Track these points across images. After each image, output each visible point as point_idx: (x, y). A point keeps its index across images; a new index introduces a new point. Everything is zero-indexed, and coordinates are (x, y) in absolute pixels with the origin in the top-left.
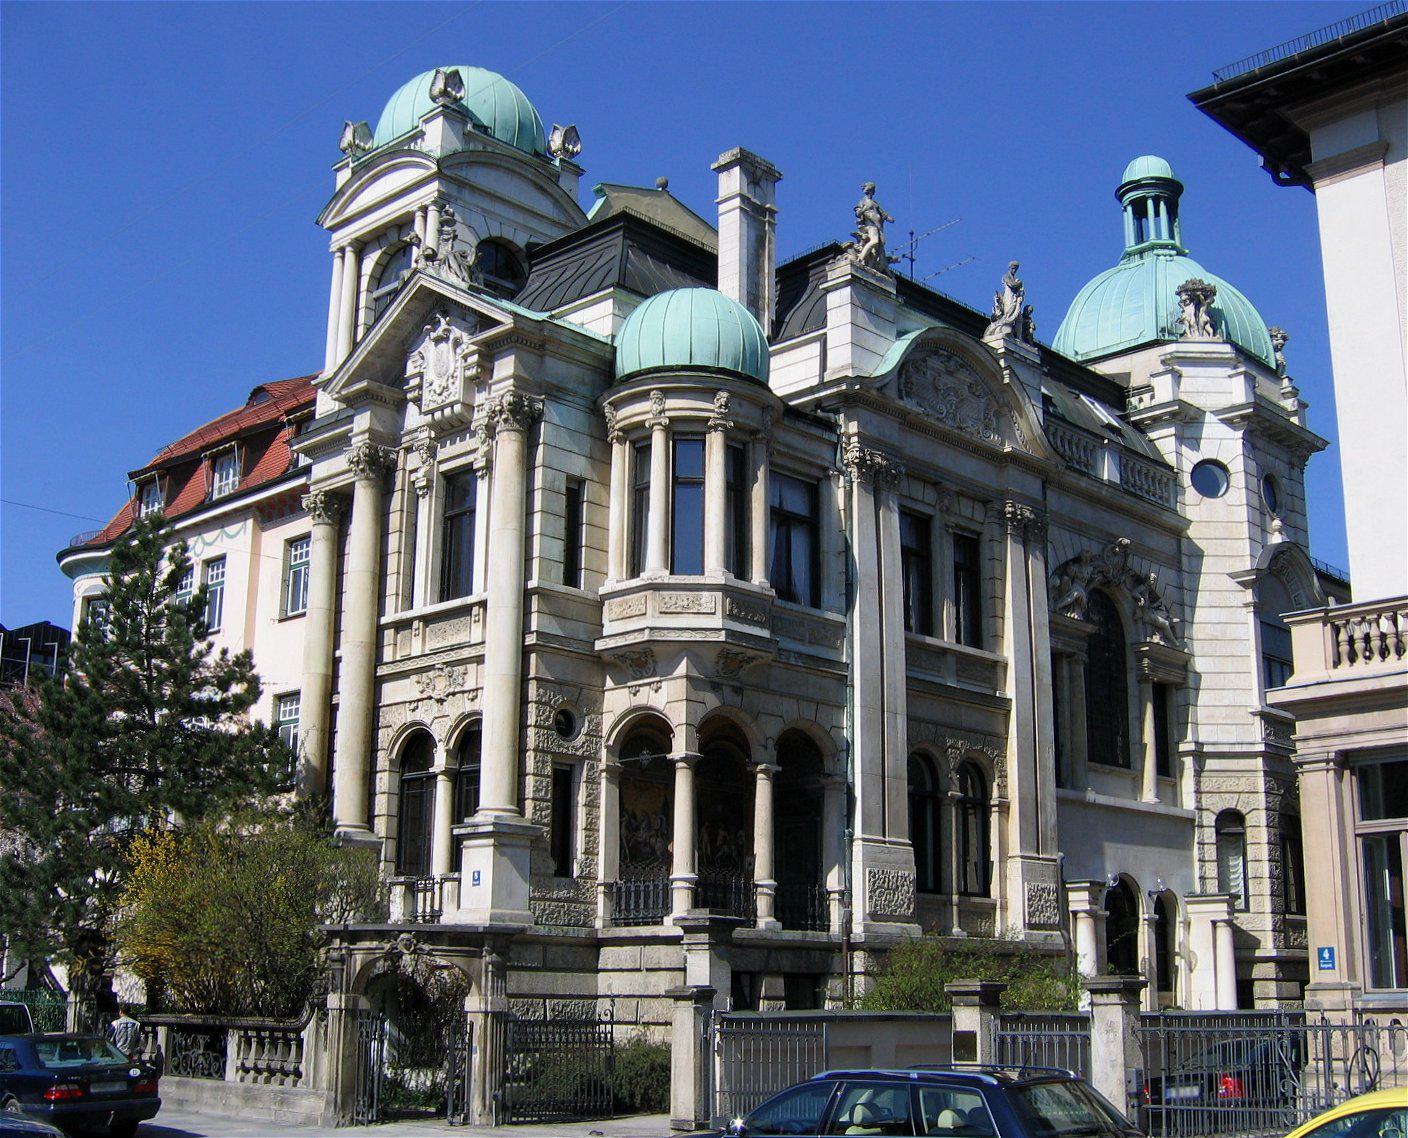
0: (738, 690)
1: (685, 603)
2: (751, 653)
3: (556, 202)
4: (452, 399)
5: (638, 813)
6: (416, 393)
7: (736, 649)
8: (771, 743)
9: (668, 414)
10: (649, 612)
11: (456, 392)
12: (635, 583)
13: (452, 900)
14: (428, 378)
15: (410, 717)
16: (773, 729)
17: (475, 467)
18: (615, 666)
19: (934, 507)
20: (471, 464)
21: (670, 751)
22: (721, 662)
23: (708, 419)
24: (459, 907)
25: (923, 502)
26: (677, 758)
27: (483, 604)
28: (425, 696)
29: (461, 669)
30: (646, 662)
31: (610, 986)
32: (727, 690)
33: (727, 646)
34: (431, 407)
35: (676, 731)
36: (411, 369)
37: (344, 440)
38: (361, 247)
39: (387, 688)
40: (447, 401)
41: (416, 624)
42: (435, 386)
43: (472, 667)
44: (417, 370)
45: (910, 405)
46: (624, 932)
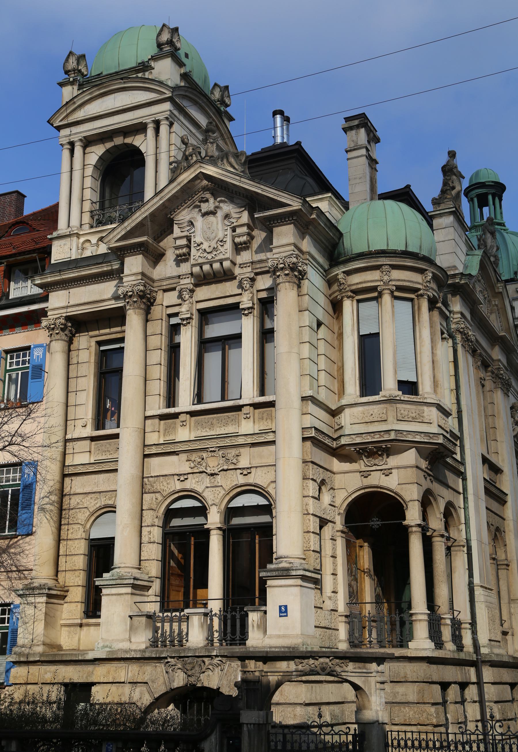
4: (221, 257)
9: (394, 283)
10: (390, 419)
15: (179, 486)
17: (241, 307)
20: (239, 303)
23: (419, 289)
24: (265, 631)
26: (413, 524)
29: (233, 452)
35: (410, 505)
37: (117, 274)
38: (88, 142)
42: (205, 246)
43: (245, 451)
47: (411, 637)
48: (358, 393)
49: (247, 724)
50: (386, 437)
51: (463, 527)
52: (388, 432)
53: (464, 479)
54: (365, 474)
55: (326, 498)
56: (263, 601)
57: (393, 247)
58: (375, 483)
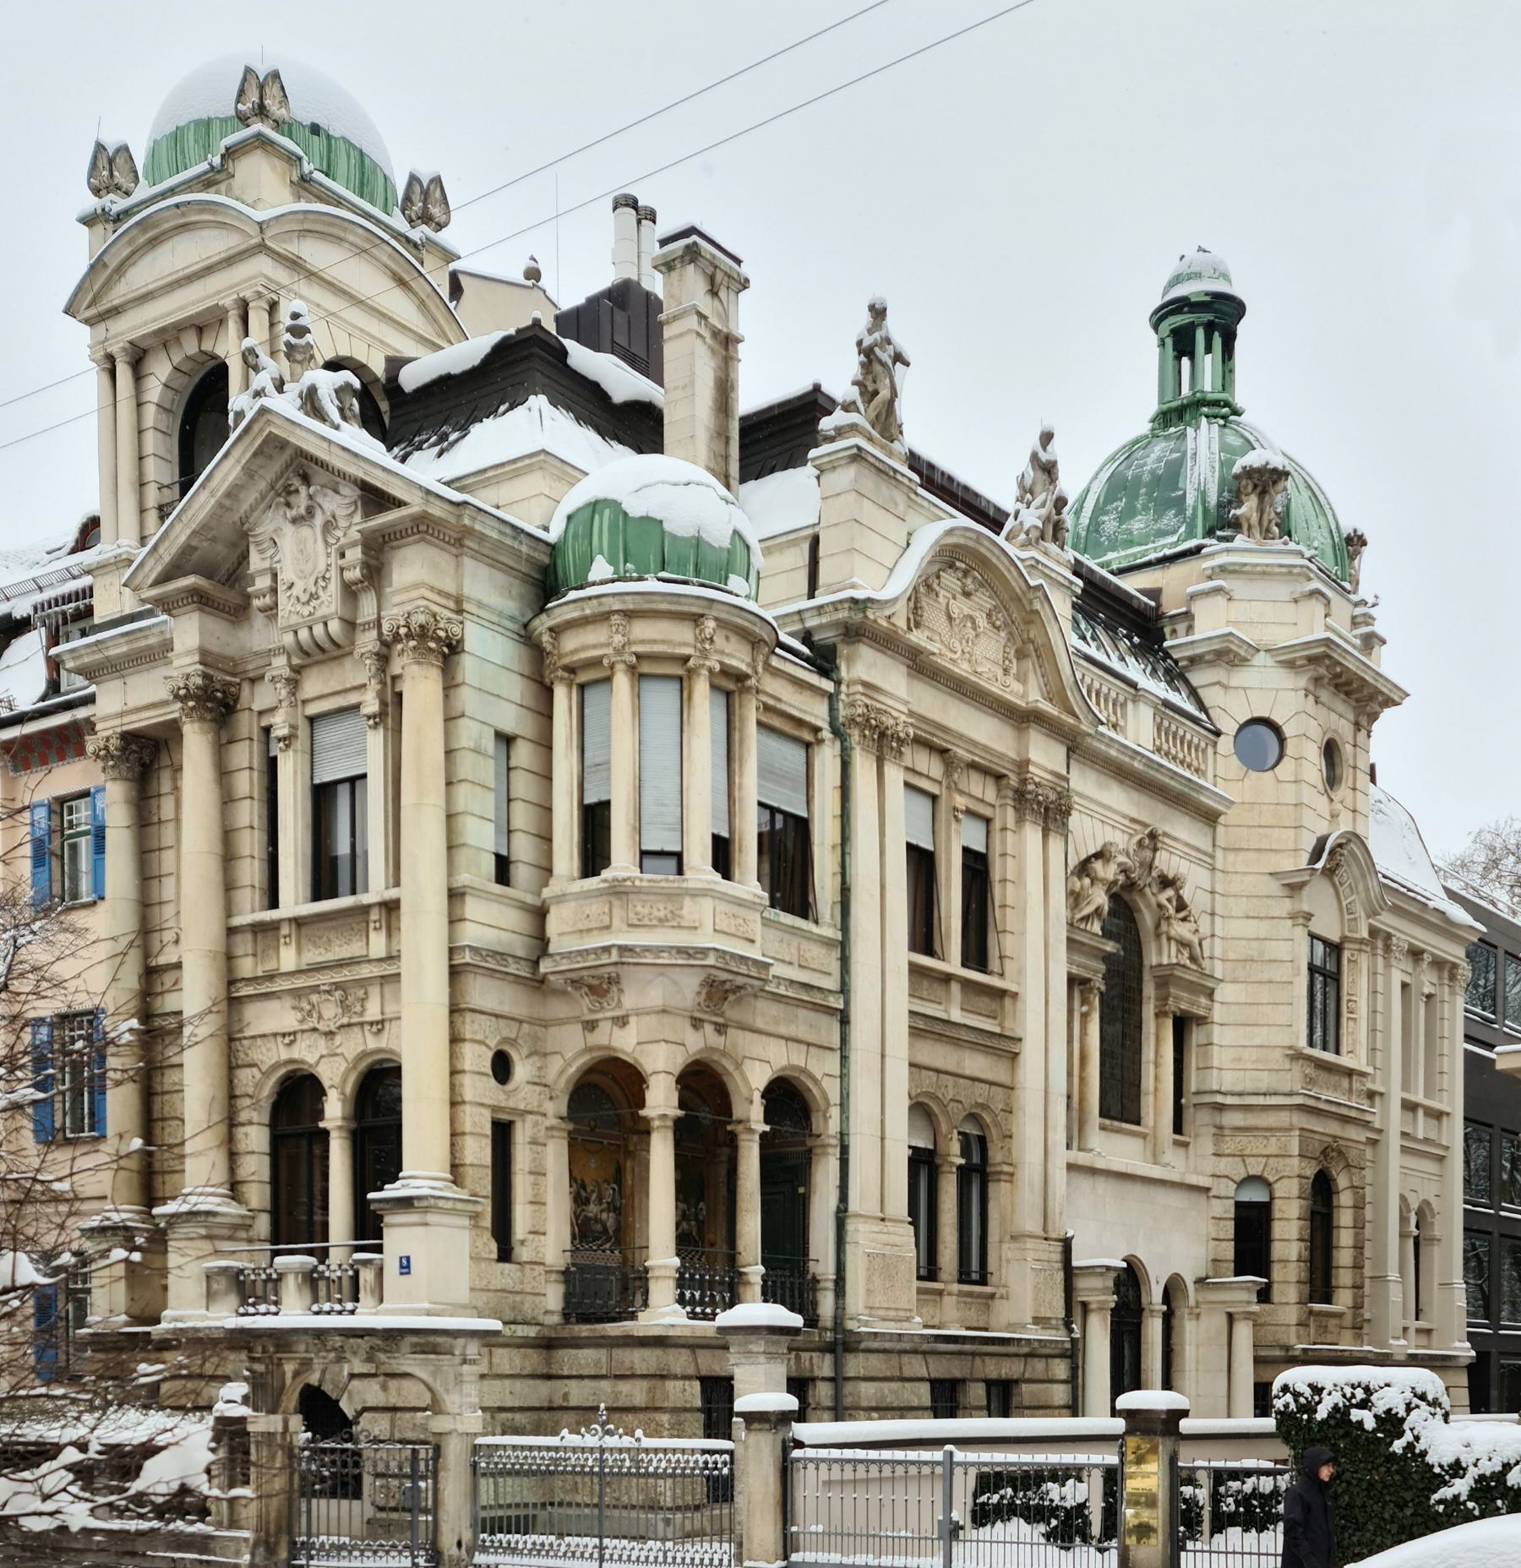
0: (721, 1029)
1: (662, 914)
2: (740, 980)
3: (422, 305)
5: (587, 1181)
6: (268, 600)
7: (724, 976)
8: (757, 1097)
10: (617, 922)
11: (331, 601)
12: (593, 883)
13: (372, 1292)
14: (285, 576)
16: (757, 1078)
18: (564, 993)
19: (940, 783)
21: (642, 1105)
22: (704, 991)
25: (928, 777)
27: (391, 907)
28: (305, 1027)
30: (608, 991)
31: (566, 1396)
32: (709, 1029)
33: (714, 972)
34: (294, 619)
36: (256, 562)
39: (251, 1011)
40: (319, 613)
41: (285, 930)
44: (266, 564)
45: (917, 638)
46: (584, 1330)
48: (576, 872)
50: (605, 960)
51: (835, 1112)
52: (606, 949)
53: (845, 1020)
54: (591, 1026)
58: (604, 1041)
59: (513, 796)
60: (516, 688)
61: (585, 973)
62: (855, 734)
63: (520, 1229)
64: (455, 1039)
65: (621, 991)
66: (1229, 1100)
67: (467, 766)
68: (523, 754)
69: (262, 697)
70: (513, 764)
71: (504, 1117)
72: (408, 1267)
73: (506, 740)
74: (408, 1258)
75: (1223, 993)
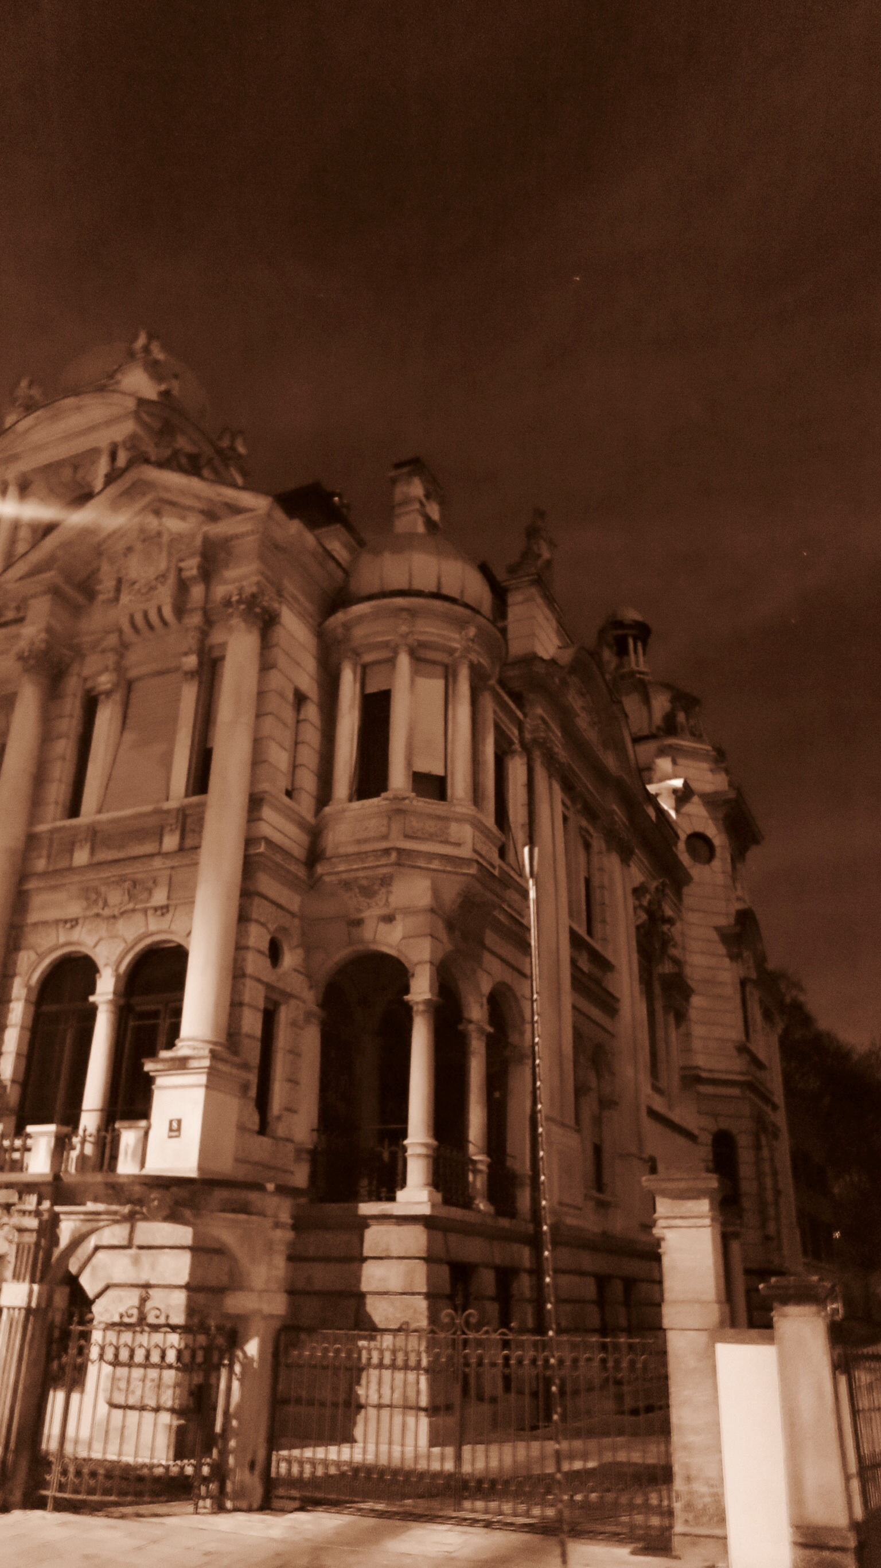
1: (432, 830)
10: (394, 834)
47: (403, 1184)
49: (9, 1308)
55: (290, 959)
56: (145, 1115)
57: (417, 585)
59: (300, 739)
60: (310, 664)
61: (361, 874)
62: (537, 754)
63: (276, 1105)
64: (243, 918)
65: (389, 892)
66: (704, 1075)
67: (273, 703)
68: (312, 712)
69: (92, 664)
70: (302, 717)
71: (275, 996)
72: (179, 1129)
73: (300, 699)
74: (179, 1122)
75: (696, 1001)
